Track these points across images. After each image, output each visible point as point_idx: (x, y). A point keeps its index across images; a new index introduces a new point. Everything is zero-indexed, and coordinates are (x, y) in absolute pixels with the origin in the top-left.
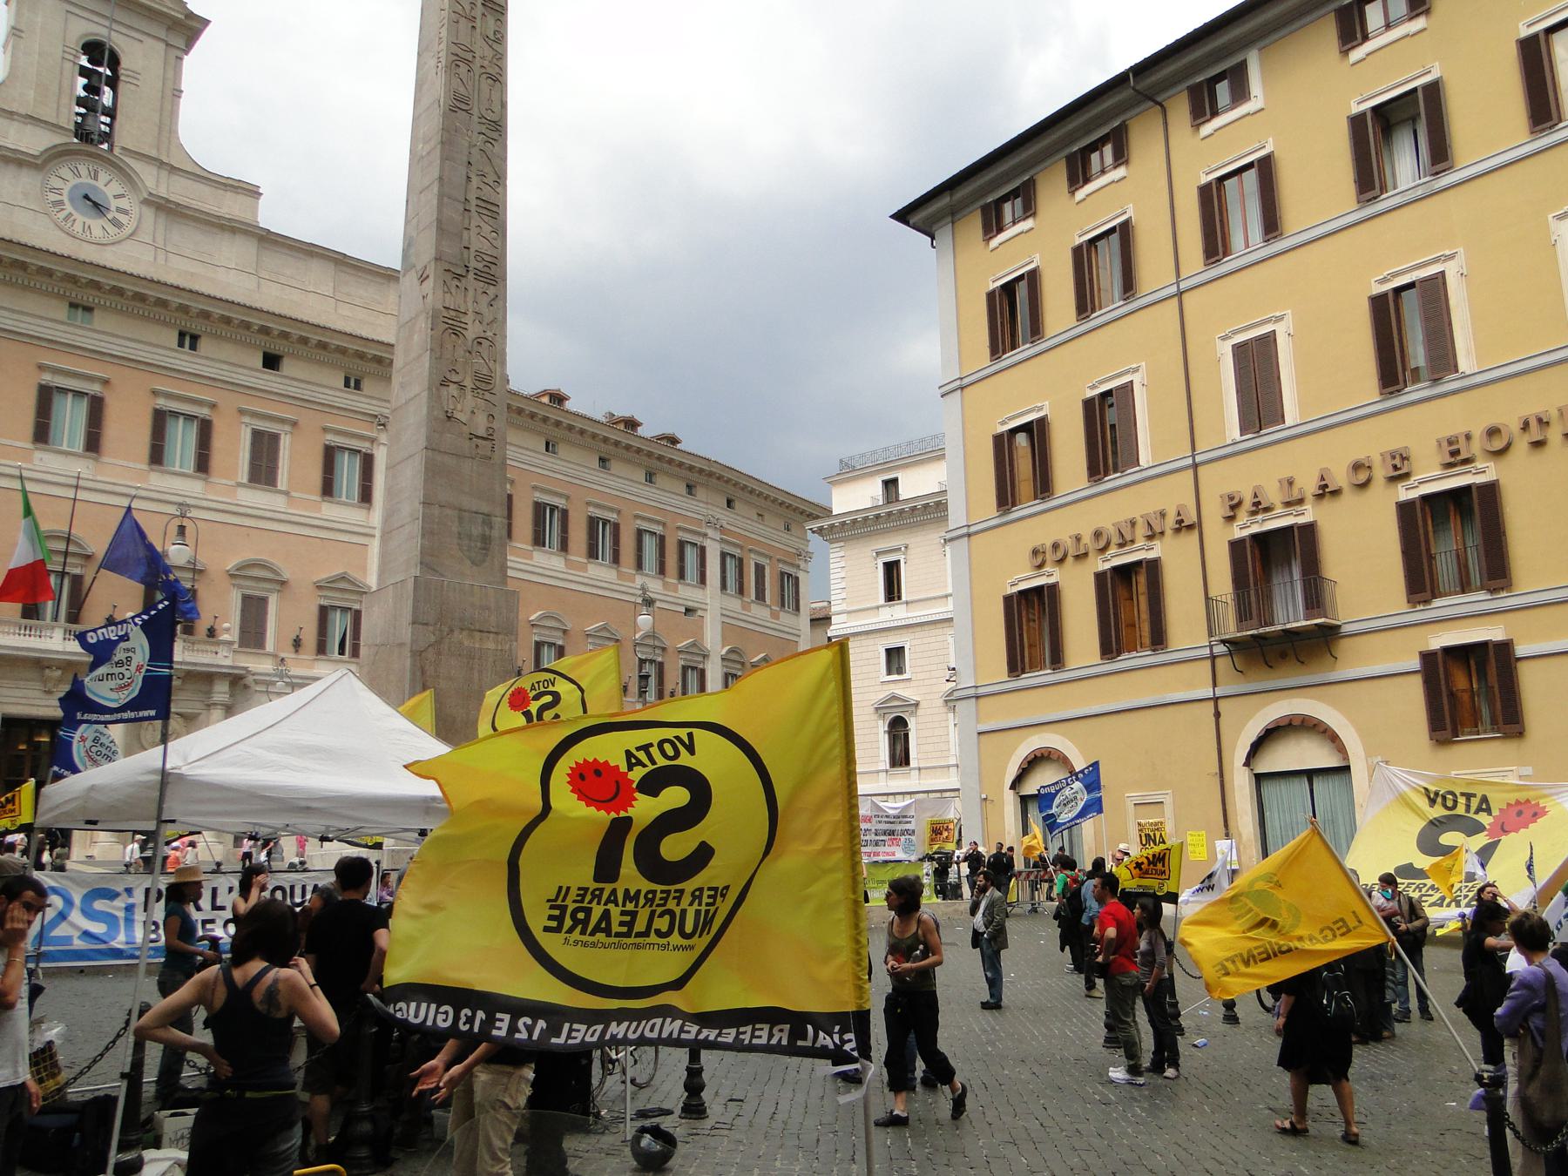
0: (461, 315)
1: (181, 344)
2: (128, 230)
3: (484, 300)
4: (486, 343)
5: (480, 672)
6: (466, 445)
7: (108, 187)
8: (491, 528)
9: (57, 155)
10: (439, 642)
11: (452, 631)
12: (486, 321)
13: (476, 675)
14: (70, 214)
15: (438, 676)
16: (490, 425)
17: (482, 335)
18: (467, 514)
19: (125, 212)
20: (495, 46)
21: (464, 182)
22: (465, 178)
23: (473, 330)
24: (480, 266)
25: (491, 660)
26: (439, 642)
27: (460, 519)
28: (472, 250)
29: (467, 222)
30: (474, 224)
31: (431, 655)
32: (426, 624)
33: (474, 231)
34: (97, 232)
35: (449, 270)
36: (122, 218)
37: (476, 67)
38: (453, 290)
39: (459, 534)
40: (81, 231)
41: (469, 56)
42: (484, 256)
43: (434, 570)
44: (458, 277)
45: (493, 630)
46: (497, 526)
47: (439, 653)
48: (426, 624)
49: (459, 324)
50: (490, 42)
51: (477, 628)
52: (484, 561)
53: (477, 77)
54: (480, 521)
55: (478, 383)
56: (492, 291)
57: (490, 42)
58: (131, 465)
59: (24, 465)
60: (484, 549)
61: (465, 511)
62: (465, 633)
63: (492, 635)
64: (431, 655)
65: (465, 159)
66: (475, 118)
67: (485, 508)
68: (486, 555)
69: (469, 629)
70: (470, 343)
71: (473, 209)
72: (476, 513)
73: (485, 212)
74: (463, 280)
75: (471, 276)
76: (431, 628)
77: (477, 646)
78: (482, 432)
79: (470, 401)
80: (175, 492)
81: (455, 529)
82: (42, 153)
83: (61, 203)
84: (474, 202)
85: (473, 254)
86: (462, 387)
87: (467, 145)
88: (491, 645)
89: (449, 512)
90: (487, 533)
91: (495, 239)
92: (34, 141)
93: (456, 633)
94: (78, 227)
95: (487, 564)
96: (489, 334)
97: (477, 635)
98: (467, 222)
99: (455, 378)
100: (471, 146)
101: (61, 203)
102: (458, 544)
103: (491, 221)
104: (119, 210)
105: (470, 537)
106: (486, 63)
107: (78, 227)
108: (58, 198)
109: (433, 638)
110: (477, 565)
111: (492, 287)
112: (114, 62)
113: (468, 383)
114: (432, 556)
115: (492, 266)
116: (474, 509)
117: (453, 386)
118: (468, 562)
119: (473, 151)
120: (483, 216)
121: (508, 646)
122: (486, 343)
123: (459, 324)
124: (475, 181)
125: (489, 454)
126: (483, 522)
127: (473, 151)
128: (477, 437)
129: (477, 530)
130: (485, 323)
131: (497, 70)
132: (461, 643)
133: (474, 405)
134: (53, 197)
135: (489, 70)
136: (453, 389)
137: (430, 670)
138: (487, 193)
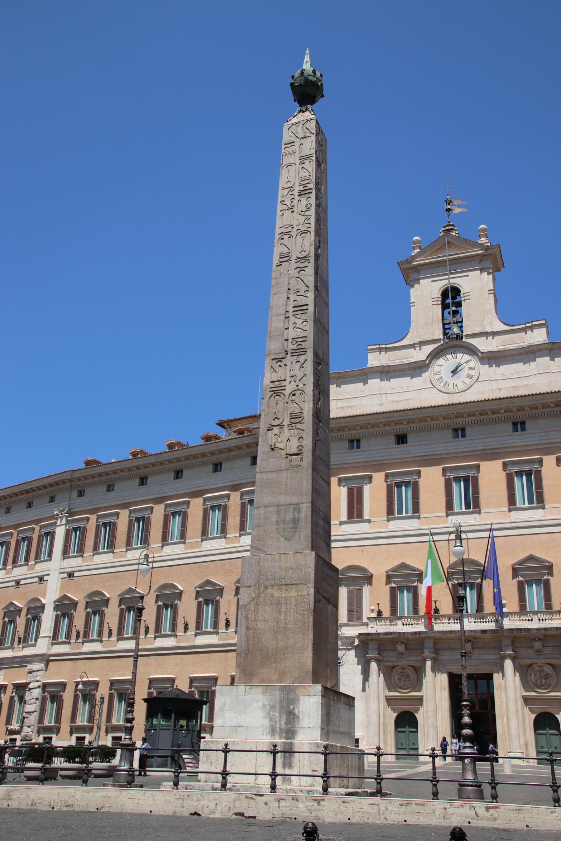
0: (282, 382)
1: (516, 430)
2: (476, 378)
3: (299, 365)
4: (298, 393)
5: (286, 613)
6: (283, 463)
7: (462, 358)
8: (299, 512)
9: (435, 355)
10: (258, 597)
11: (266, 588)
12: (299, 378)
13: (283, 615)
14: (446, 382)
15: (257, 621)
16: (300, 444)
17: (296, 388)
18: (283, 508)
19: (473, 368)
20: (307, 213)
21: (285, 302)
22: (286, 299)
23: (290, 388)
24: (295, 347)
25: (293, 604)
26: (258, 597)
27: (278, 513)
28: (290, 341)
29: (287, 323)
30: (291, 323)
31: (252, 607)
32: (250, 587)
33: (291, 327)
34: (461, 386)
35: (275, 359)
36: (472, 372)
37: (294, 233)
38: (277, 370)
39: (277, 521)
40: (452, 389)
41: (289, 229)
42: (298, 340)
43: (261, 550)
44: (280, 360)
45: (294, 582)
46: (304, 509)
47: (257, 605)
48: (250, 587)
49: (280, 388)
50: (303, 213)
51: (284, 583)
52: (294, 536)
53: (294, 238)
54: (292, 509)
55: (293, 421)
56: (302, 358)
57: (303, 213)
58: (499, 510)
59: (431, 527)
60: (294, 528)
61: (281, 506)
62: (275, 588)
63: (294, 586)
64: (252, 607)
65: (286, 288)
66: (293, 261)
67: (295, 500)
68: (296, 531)
69: (279, 585)
70: (287, 396)
71: (290, 314)
72: (289, 505)
73: (299, 312)
74: (284, 360)
75: (289, 354)
76: (252, 589)
77: (284, 595)
78: (294, 451)
79: (286, 433)
80: (538, 519)
81: (274, 519)
82: (427, 357)
83: (441, 378)
84: (291, 309)
85: (290, 341)
86: (280, 426)
87: (287, 279)
88: (293, 593)
89: (270, 509)
90: (297, 516)
91: (305, 326)
92: (420, 355)
93: (269, 589)
94: (451, 387)
95: (296, 537)
96: (301, 386)
97: (284, 587)
98: (287, 323)
99: (277, 422)
100: (289, 279)
101: (441, 378)
102: (277, 529)
103: (303, 316)
104: (469, 369)
105: (284, 522)
106: (299, 227)
107: (451, 387)
108: (440, 376)
109: (253, 595)
110: (288, 540)
111: (302, 356)
112: (456, 291)
113: (286, 422)
114: (259, 540)
115: (303, 343)
116: (288, 503)
117: (275, 428)
118: (283, 539)
119: (291, 281)
120: (299, 316)
121: (306, 592)
122: (298, 393)
123: (280, 388)
124: (292, 297)
125: (299, 463)
126: (294, 509)
127: (291, 281)
128: (291, 455)
129: (289, 516)
130: (297, 381)
131: (308, 225)
132: (273, 596)
133: (289, 435)
134: (437, 377)
135: (303, 229)
136: (276, 430)
137: (251, 617)
138: (301, 300)
